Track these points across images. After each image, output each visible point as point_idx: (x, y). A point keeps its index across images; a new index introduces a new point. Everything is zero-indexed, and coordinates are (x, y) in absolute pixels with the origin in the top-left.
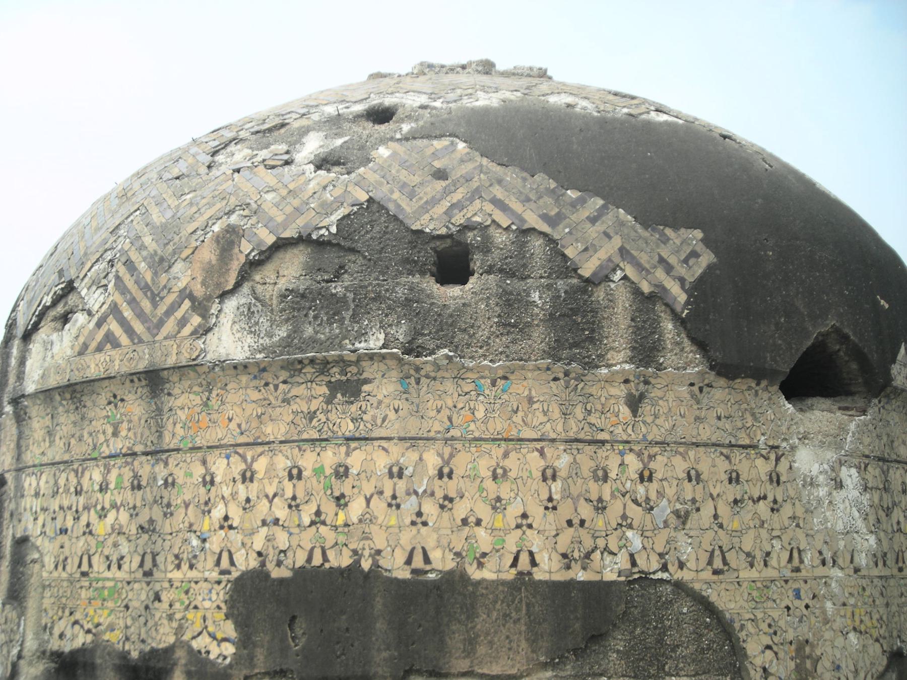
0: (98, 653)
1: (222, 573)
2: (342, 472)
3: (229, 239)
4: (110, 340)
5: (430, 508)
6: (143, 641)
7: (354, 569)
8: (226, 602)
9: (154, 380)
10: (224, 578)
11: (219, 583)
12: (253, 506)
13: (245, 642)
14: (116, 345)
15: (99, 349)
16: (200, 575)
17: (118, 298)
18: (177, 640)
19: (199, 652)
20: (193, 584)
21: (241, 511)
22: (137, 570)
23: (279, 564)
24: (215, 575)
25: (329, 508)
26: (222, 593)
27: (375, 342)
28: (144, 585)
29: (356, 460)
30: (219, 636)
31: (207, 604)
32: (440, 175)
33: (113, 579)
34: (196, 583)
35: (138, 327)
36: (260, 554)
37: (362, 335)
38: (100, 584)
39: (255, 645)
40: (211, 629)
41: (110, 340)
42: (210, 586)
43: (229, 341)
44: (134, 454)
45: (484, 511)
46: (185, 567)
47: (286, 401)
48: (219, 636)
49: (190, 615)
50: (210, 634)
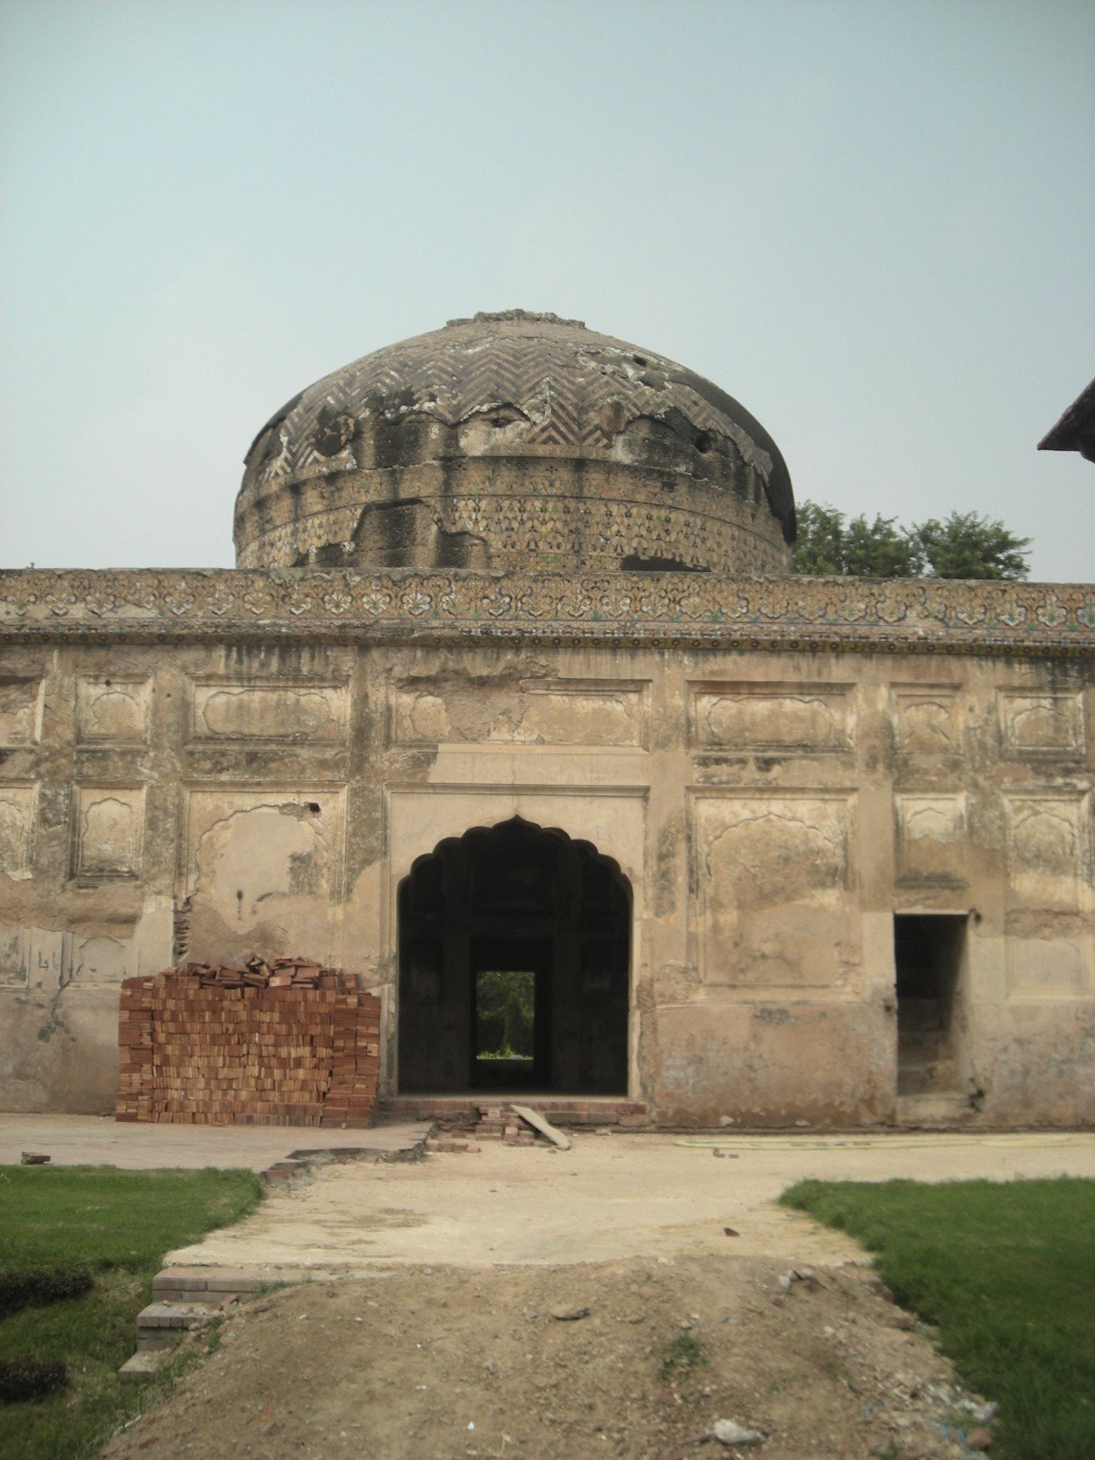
3: (617, 408)
4: (551, 438)
5: (698, 541)
7: (674, 559)
9: (580, 465)
14: (556, 442)
15: (544, 442)
17: (554, 419)
25: (663, 534)
29: (673, 516)
32: (696, 403)
35: (571, 437)
37: (677, 465)
43: (620, 453)
44: (565, 497)
45: (715, 546)
47: (645, 486)
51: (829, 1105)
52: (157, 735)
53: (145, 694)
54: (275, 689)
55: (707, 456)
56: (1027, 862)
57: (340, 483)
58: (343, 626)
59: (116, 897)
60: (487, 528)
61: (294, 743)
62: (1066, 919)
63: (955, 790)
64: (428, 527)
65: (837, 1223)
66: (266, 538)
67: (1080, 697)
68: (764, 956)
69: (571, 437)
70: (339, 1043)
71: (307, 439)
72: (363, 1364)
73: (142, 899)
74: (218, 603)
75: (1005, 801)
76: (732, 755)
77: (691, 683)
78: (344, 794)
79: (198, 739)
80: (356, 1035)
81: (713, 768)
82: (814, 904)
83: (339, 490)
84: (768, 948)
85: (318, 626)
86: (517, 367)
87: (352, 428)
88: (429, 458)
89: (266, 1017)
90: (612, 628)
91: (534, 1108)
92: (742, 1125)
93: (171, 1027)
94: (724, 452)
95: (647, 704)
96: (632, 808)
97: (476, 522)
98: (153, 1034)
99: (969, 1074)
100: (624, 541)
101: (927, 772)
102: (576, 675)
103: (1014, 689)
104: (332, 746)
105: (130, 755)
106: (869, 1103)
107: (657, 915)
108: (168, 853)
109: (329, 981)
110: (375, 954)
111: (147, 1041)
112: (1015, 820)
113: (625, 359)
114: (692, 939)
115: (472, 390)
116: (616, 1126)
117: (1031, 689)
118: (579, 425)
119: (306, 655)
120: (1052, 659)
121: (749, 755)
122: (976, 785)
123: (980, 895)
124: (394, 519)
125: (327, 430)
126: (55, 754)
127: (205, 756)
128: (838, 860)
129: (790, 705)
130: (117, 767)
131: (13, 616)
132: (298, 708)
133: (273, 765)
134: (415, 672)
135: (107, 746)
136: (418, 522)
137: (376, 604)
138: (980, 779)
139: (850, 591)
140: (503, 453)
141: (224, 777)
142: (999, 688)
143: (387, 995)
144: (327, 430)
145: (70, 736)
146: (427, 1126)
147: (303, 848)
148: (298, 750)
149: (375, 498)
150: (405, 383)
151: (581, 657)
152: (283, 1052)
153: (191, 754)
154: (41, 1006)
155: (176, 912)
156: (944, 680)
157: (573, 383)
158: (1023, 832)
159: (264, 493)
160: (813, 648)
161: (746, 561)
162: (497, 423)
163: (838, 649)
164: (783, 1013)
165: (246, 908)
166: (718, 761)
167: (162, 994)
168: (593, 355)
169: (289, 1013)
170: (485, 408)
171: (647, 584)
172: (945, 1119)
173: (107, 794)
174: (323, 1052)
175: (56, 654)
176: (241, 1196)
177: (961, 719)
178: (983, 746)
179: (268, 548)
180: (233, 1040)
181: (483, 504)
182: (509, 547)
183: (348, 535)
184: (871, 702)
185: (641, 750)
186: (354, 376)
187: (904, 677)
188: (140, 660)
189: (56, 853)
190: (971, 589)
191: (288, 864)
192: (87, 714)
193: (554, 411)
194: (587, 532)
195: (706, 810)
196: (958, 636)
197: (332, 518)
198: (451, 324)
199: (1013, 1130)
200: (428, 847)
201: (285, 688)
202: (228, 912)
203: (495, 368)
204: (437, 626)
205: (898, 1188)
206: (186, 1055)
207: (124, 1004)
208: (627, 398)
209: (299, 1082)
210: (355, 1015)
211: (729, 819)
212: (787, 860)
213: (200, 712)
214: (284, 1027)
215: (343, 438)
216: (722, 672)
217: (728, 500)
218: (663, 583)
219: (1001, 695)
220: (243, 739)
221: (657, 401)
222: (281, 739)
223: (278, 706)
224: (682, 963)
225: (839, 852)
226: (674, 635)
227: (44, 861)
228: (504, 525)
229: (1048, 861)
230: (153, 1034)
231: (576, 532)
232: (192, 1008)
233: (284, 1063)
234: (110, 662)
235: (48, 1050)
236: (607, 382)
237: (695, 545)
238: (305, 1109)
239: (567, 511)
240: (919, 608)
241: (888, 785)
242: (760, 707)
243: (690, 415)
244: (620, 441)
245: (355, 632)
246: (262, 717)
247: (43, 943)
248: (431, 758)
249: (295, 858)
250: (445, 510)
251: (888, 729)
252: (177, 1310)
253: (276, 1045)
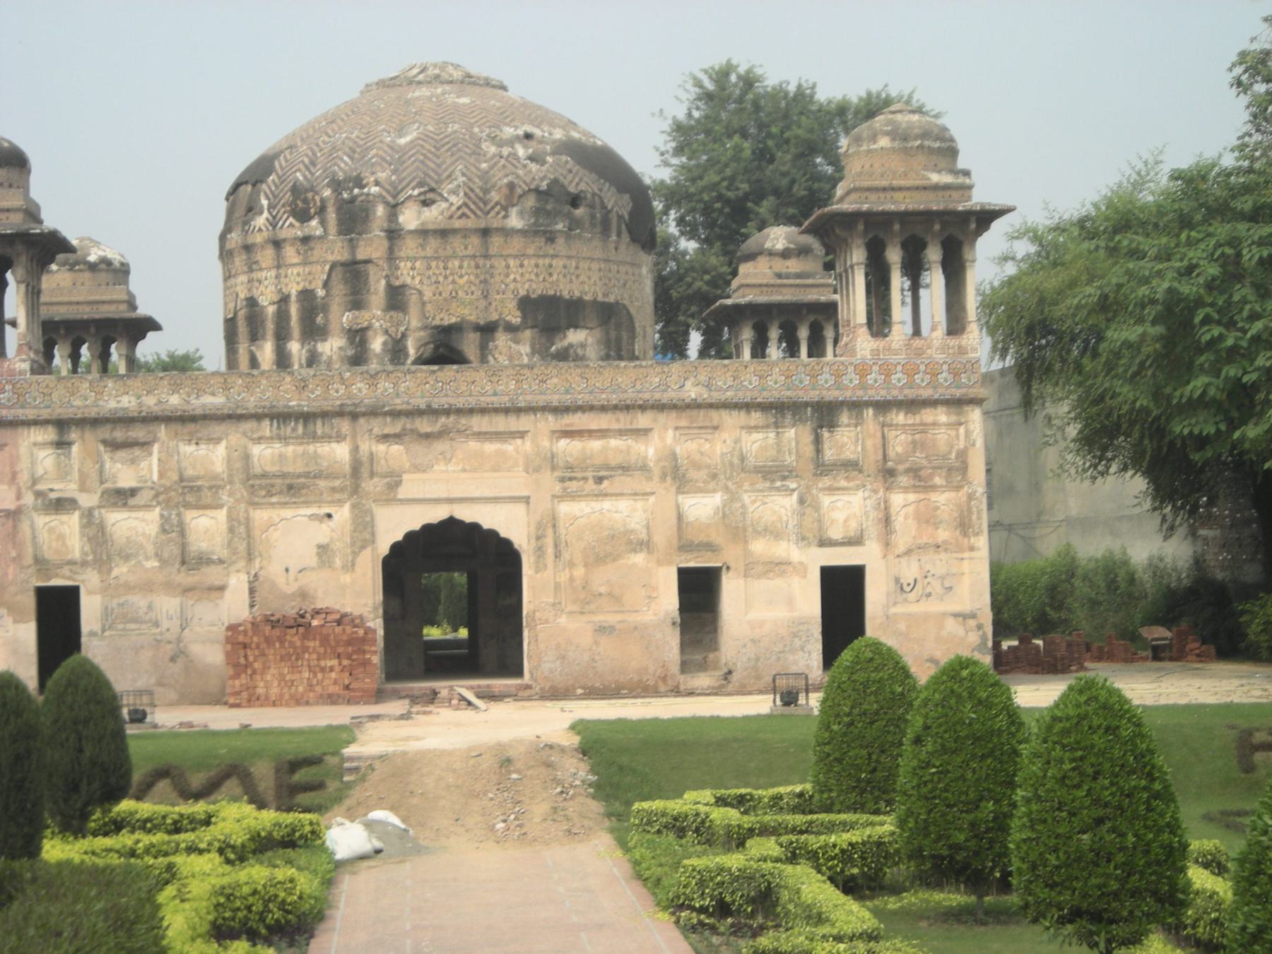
2: (551, 266)
3: (511, 186)
9: (485, 233)
14: (468, 217)
15: (460, 217)
27: (560, 226)
29: (554, 262)
32: (570, 171)
35: (478, 212)
41: (464, 215)
43: (515, 221)
51: (640, 681)
52: (231, 475)
53: (221, 450)
54: (302, 444)
55: (580, 212)
56: (760, 533)
57: (312, 244)
58: (342, 405)
59: (212, 575)
60: (421, 282)
61: (315, 477)
62: (783, 567)
63: (714, 491)
64: (378, 281)
65: (579, 733)
66: (254, 275)
67: (793, 431)
68: (600, 594)
69: (478, 212)
70: (355, 657)
71: (283, 206)
72: (419, 769)
73: (228, 575)
74: (263, 392)
75: (746, 498)
76: (579, 475)
77: (554, 432)
78: (347, 507)
79: (256, 476)
80: (364, 652)
81: (568, 483)
82: (630, 562)
83: (312, 249)
84: (603, 590)
85: (327, 406)
86: (438, 157)
87: (318, 203)
88: (377, 231)
89: (311, 644)
90: (505, 401)
91: (467, 688)
92: (590, 693)
93: (257, 652)
94: (592, 206)
95: (527, 445)
96: (520, 509)
97: (413, 278)
98: (246, 656)
99: (723, 661)
100: (519, 285)
101: (697, 481)
102: (484, 429)
103: (752, 428)
104: (337, 478)
105: (215, 488)
106: (664, 679)
107: (537, 572)
108: (242, 547)
109: (346, 620)
110: (370, 602)
111: (242, 661)
112: (751, 510)
113: (517, 138)
114: (557, 586)
115: (404, 179)
116: (514, 696)
117: (763, 427)
118: (485, 203)
119: (319, 422)
120: (776, 408)
121: (590, 474)
122: (727, 488)
123: (728, 555)
124: (353, 273)
125: (299, 203)
126: (167, 490)
127: (261, 487)
128: (644, 536)
129: (614, 443)
130: (207, 497)
131: (133, 404)
132: (316, 456)
133: (304, 491)
134: (386, 431)
135: (199, 483)
137: (360, 390)
138: (730, 484)
139: (651, 371)
140: (431, 227)
141: (274, 500)
142: (742, 428)
143: (377, 624)
144: (300, 204)
145: (176, 477)
146: (407, 701)
147: (323, 540)
148: (318, 482)
149: (339, 258)
150: (356, 169)
151: (486, 419)
152: (323, 663)
153: (253, 486)
154: (170, 642)
155: (250, 582)
156: (708, 424)
157: (479, 169)
158: (756, 515)
159: (250, 241)
160: (628, 408)
161: (611, 285)
162: (426, 203)
163: (643, 408)
164: (612, 628)
165: (291, 577)
166: (571, 479)
167: (250, 633)
168: (492, 139)
169: (325, 641)
170: (416, 192)
171: (526, 371)
172: (709, 687)
173: (201, 512)
174: (346, 662)
175: (163, 427)
176: (346, 733)
177: (718, 447)
178: (731, 464)
179: (256, 284)
180: (292, 658)
181: (418, 264)
183: (320, 284)
184: (663, 439)
185: (524, 474)
186: (314, 154)
187: (683, 423)
188: (216, 429)
189: (173, 550)
190: (725, 366)
191: (315, 550)
192: (185, 464)
193: (466, 194)
195: (565, 508)
196: (716, 396)
197: (307, 270)
198: (382, 84)
199: (750, 693)
200: (399, 537)
201: (308, 443)
202: (281, 580)
203: (422, 158)
204: (399, 404)
205: (621, 723)
206: (266, 668)
207: (228, 640)
208: (518, 177)
209: (332, 680)
210: (363, 640)
211: (578, 514)
212: (613, 536)
213: (255, 460)
214: (322, 650)
215: (312, 211)
216: (571, 425)
217: (596, 243)
218: (535, 370)
219: (744, 432)
220: (284, 476)
221: (539, 174)
222: (307, 475)
223: (303, 454)
224: (552, 600)
225: (644, 531)
226: (541, 404)
227: (166, 555)
228: (433, 279)
229: (771, 532)
230: (246, 656)
231: (485, 281)
232: (268, 641)
233: (323, 670)
234: (196, 431)
235: (176, 668)
236: (504, 166)
237: (571, 281)
238: (339, 696)
239: (477, 267)
240: (692, 379)
241: (673, 489)
242: (596, 444)
243: (566, 182)
244: (514, 211)
245: (351, 408)
246: (295, 462)
247: (168, 605)
248: (398, 484)
249: (319, 547)
250: (390, 268)
251: (674, 456)
252: (354, 764)
253: (318, 659)
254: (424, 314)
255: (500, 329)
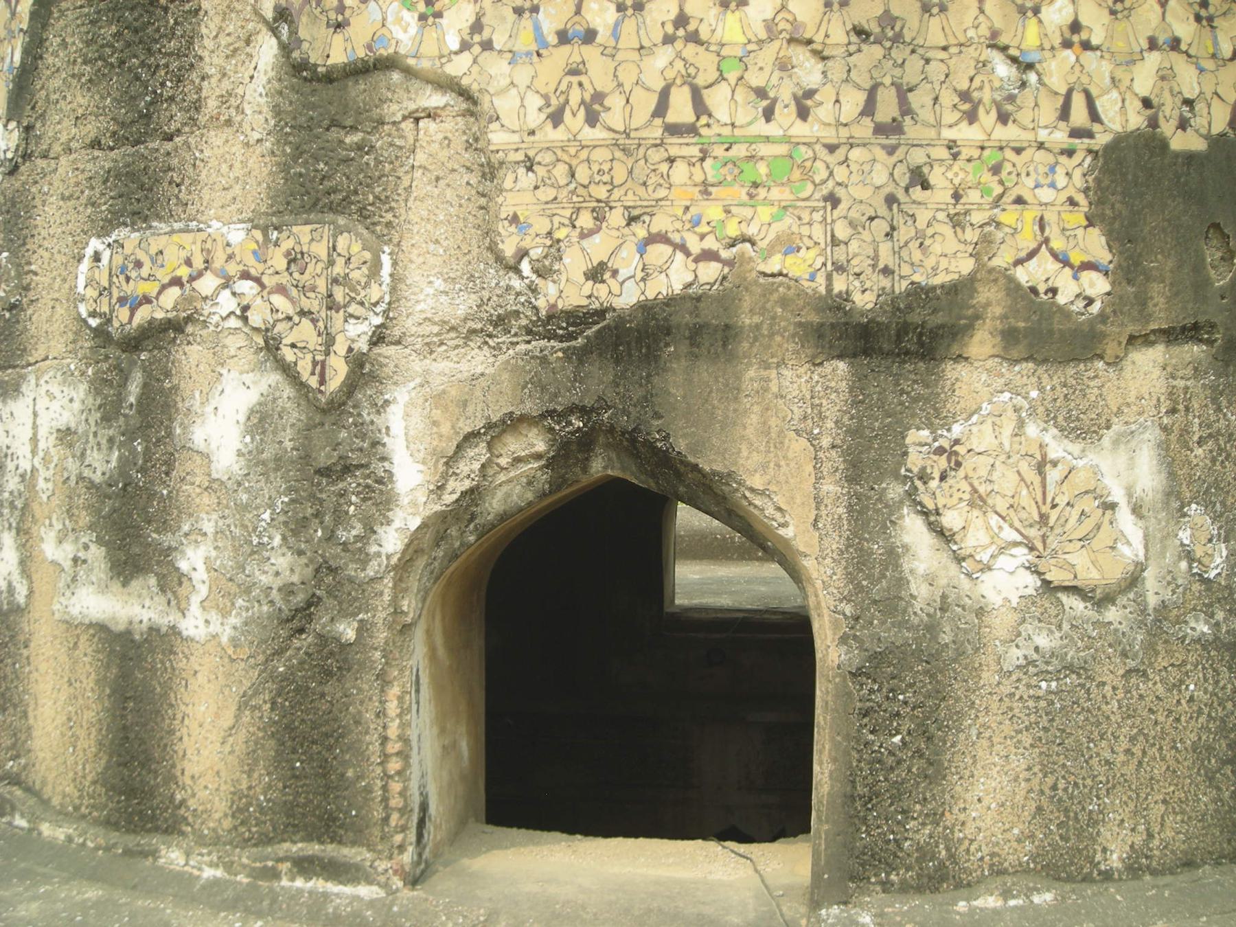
0: (747, 302)
1: (1076, 133)
6: (887, 271)
8: (1086, 191)
10: (1081, 144)
11: (1070, 153)
12: (1130, 9)
13: (1129, 270)
16: (1030, 136)
18: (980, 265)
19: (1034, 290)
20: (1009, 154)
21: (1106, 18)
22: (857, 121)
23: (1183, 125)
24: (1060, 137)
26: (1077, 174)
28: (880, 154)
30: (1076, 258)
31: (1046, 195)
33: (786, 139)
34: (1018, 151)
36: (1147, 103)
38: (739, 151)
39: (1148, 279)
40: (1057, 244)
42: (1050, 159)
46: (988, 118)
48: (1076, 258)
49: (1008, 217)
50: (1055, 255)
136: (208, 28)
182: (575, 121)
194: (934, 32)
254: (488, 233)
255: (981, 343)
